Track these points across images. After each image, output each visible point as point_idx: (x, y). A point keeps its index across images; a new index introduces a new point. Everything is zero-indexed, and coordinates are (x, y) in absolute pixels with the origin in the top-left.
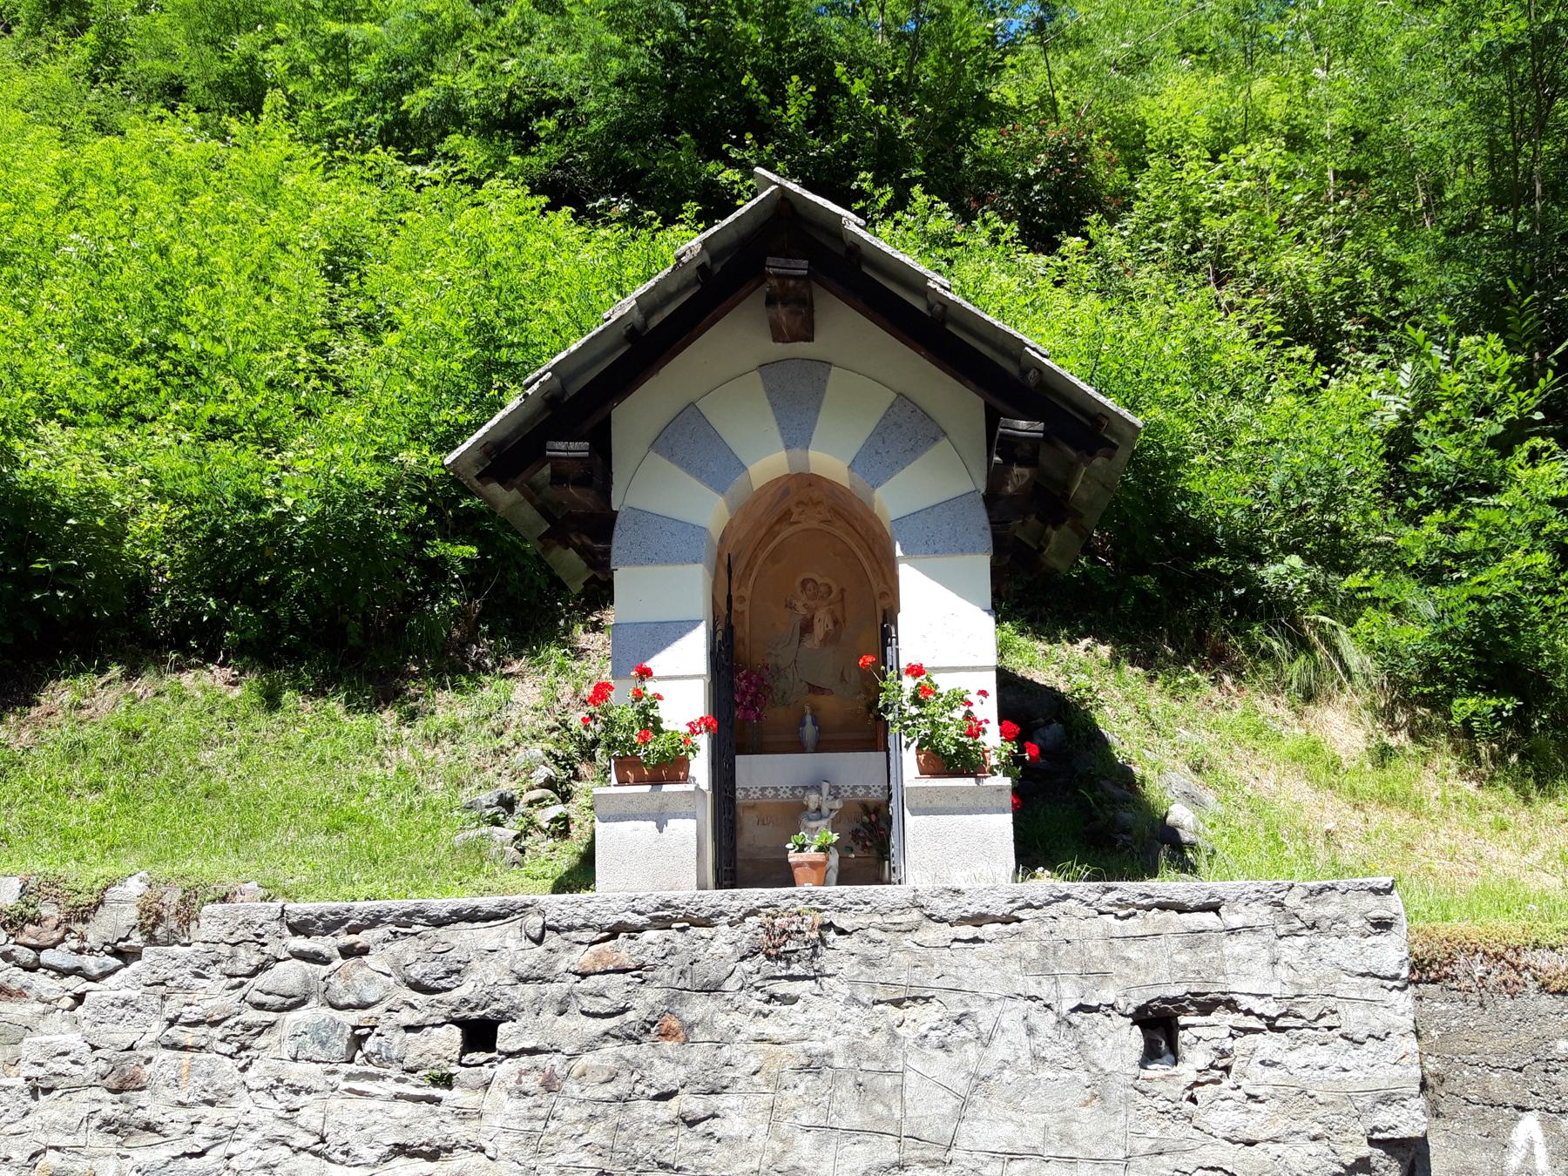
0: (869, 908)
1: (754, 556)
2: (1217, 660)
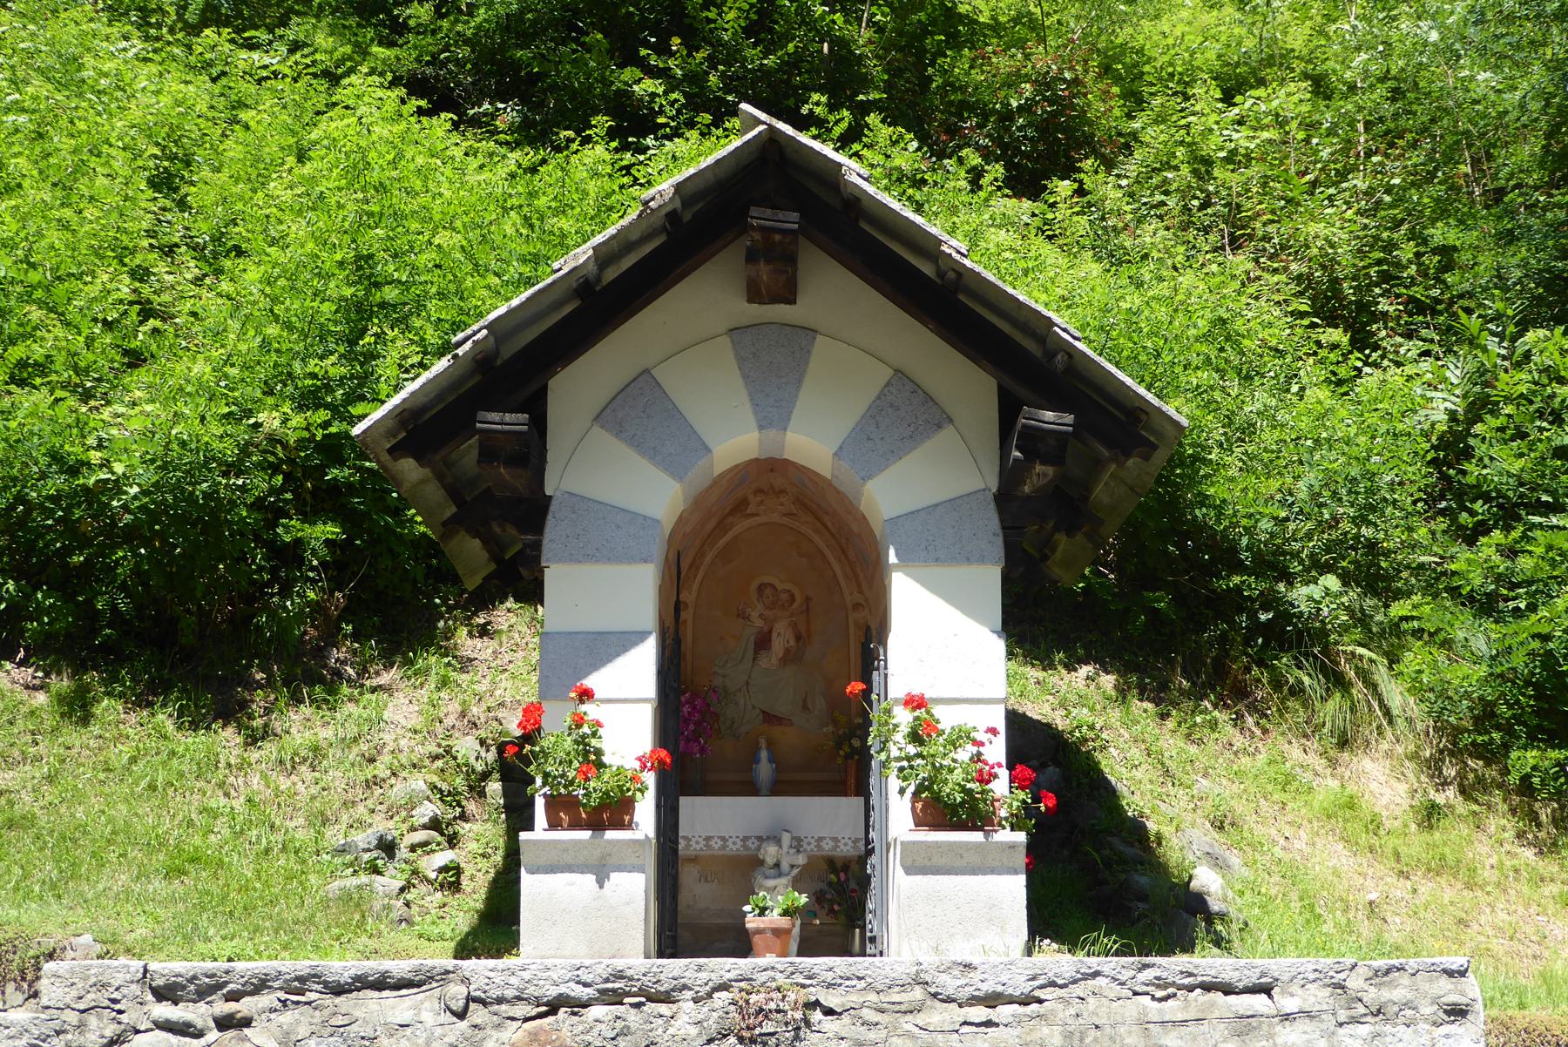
0: (862, 984)
1: (700, 554)
2: (1236, 695)
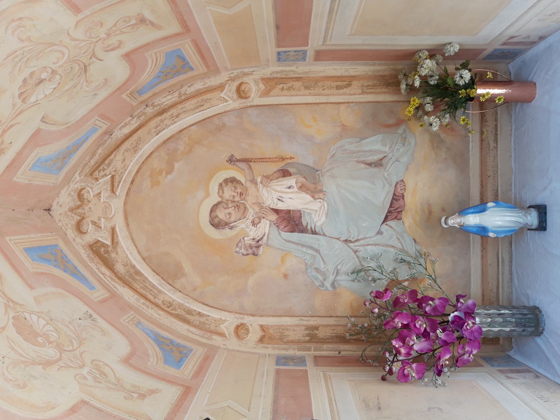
1: (168, 308)
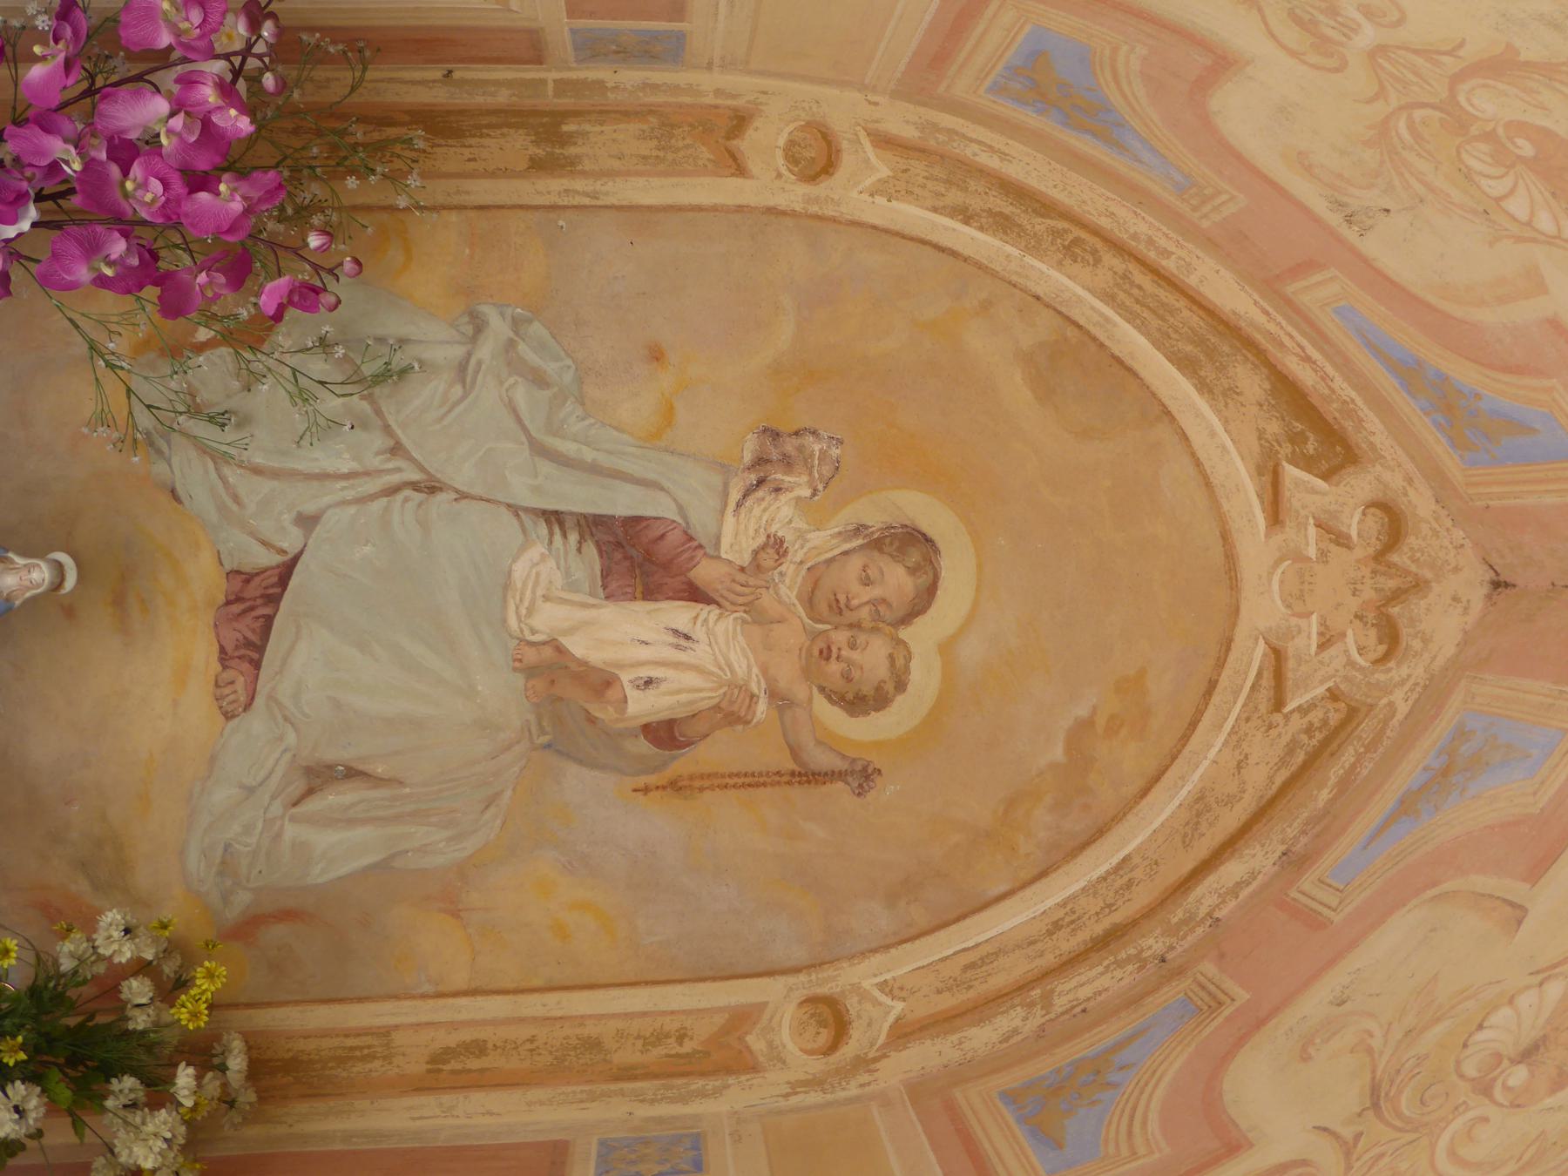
1: (1079, 239)
